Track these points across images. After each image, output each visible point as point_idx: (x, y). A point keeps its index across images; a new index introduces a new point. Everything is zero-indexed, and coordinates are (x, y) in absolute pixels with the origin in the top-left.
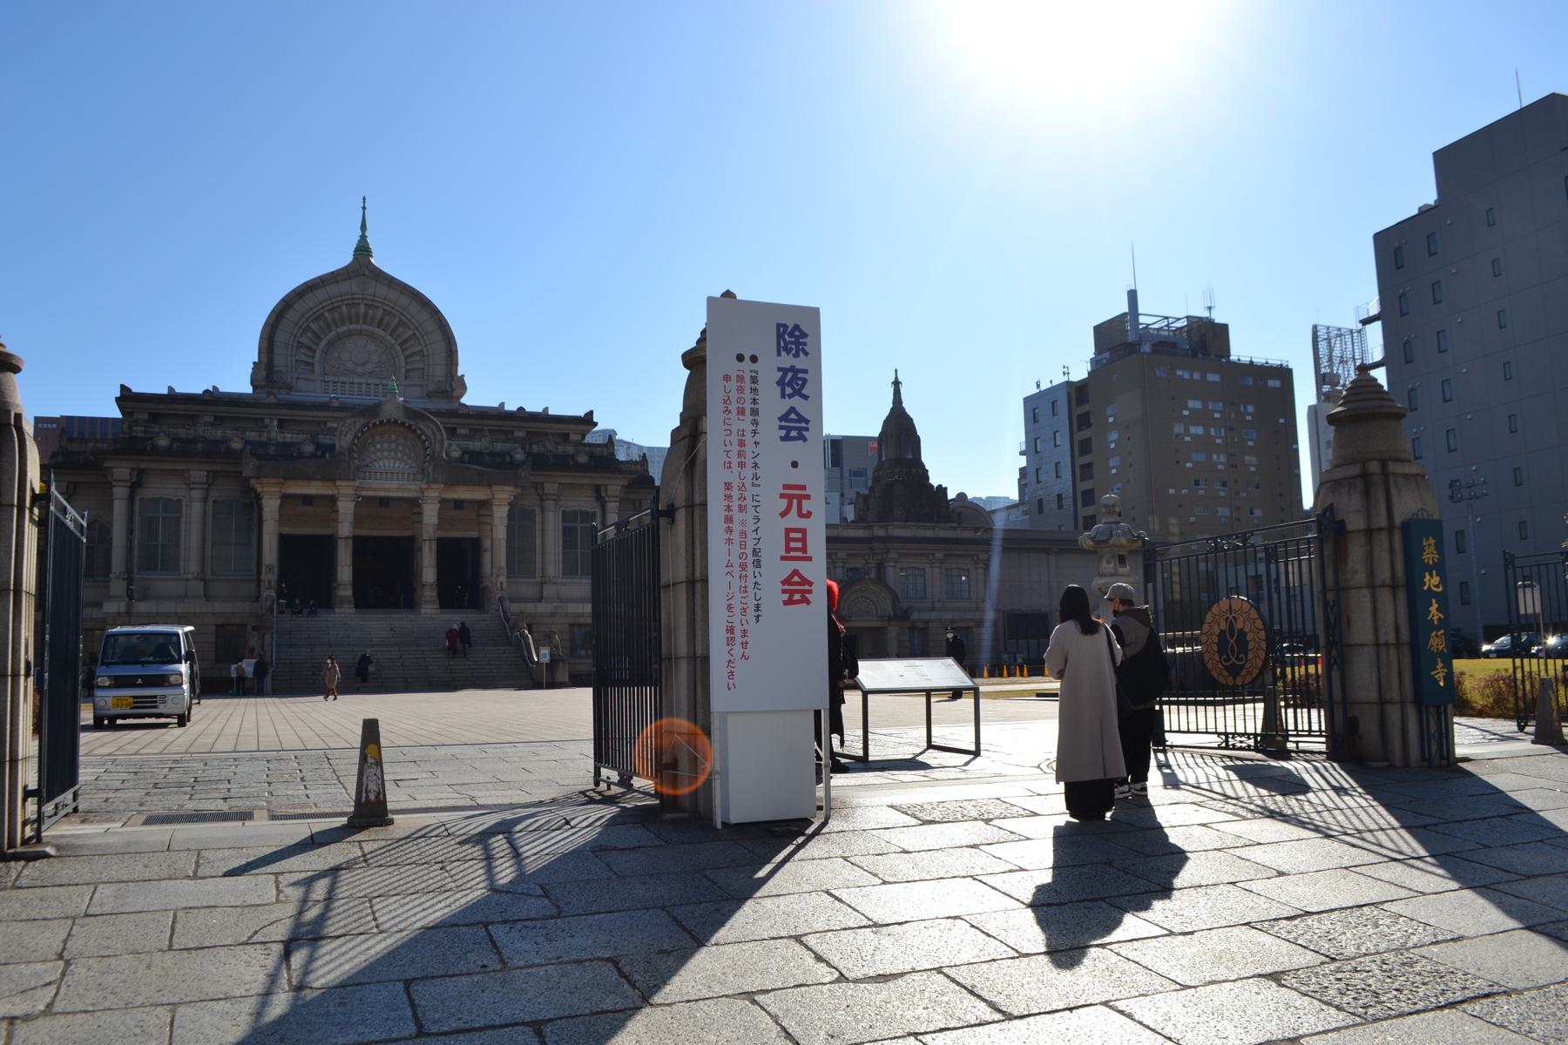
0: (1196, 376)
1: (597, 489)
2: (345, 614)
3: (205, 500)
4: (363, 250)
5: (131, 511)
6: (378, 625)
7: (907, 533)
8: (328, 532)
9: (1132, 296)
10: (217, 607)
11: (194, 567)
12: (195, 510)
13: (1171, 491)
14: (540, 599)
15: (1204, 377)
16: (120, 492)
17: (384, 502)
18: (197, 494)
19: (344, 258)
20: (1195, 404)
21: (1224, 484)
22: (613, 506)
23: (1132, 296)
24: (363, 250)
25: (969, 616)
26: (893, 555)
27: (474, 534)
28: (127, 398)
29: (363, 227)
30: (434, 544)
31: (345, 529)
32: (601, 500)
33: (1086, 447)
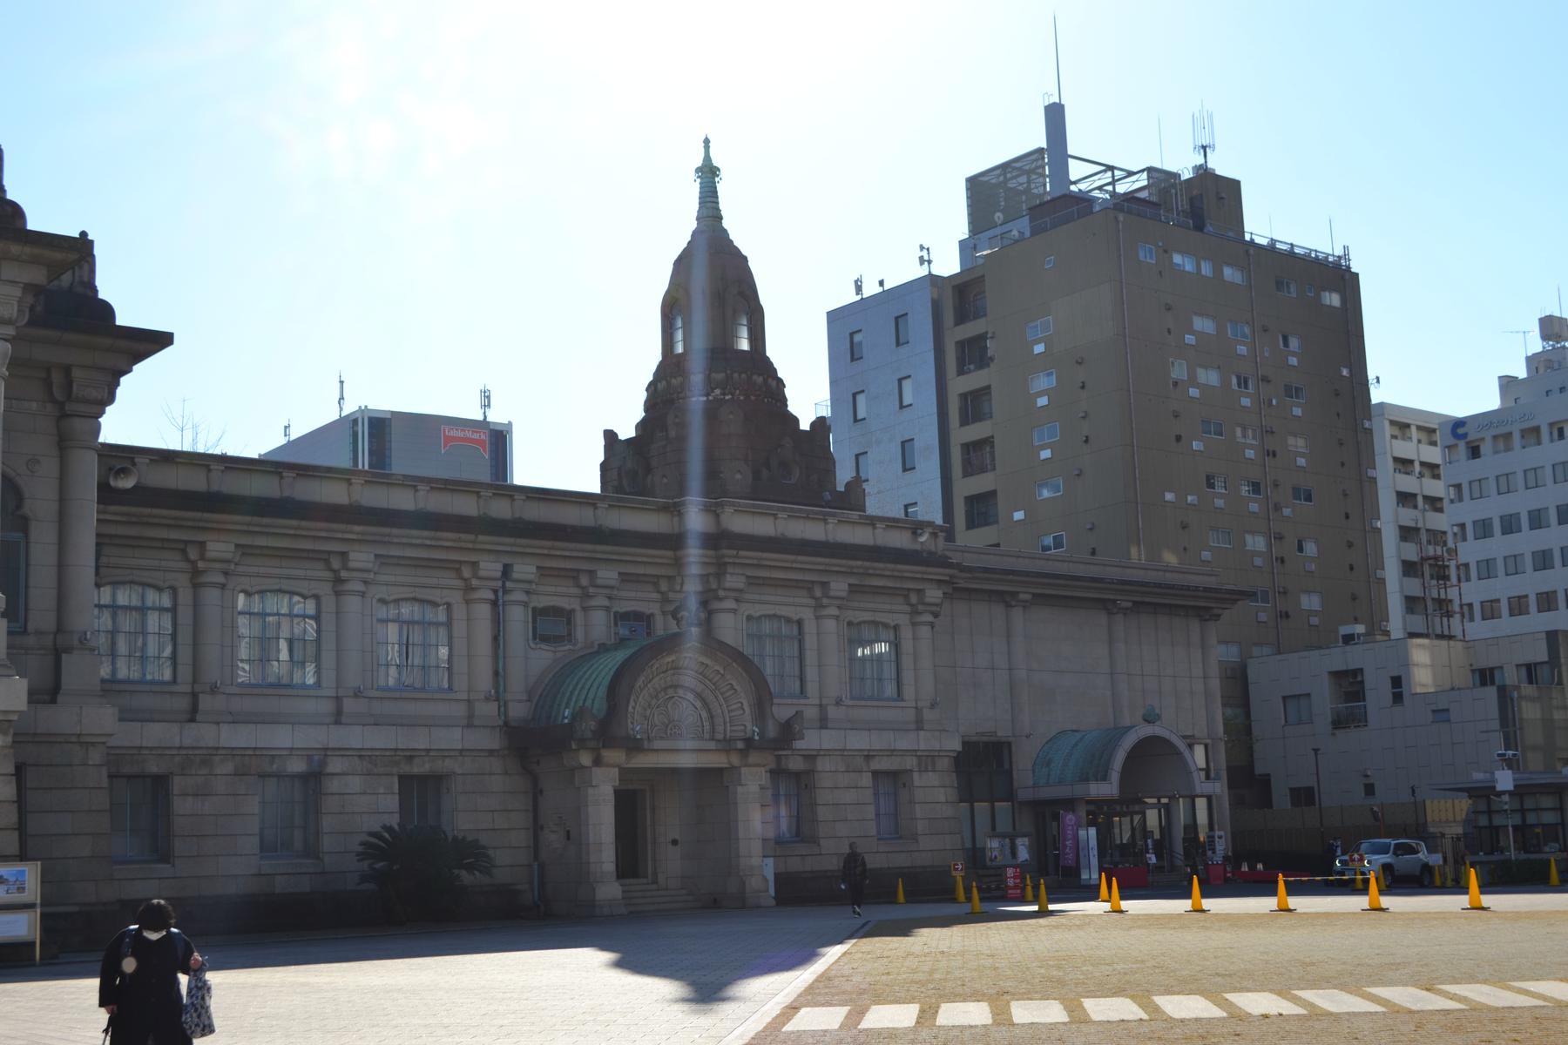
7: (762, 526)
9: (1055, 116)
13: (1169, 496)
15: (1218, 272)
20: (1203, 324)
21: (1256, 487)
23: (1055, 116)
25: (905, 742)
26: (733, 580)
33: (975, 405)
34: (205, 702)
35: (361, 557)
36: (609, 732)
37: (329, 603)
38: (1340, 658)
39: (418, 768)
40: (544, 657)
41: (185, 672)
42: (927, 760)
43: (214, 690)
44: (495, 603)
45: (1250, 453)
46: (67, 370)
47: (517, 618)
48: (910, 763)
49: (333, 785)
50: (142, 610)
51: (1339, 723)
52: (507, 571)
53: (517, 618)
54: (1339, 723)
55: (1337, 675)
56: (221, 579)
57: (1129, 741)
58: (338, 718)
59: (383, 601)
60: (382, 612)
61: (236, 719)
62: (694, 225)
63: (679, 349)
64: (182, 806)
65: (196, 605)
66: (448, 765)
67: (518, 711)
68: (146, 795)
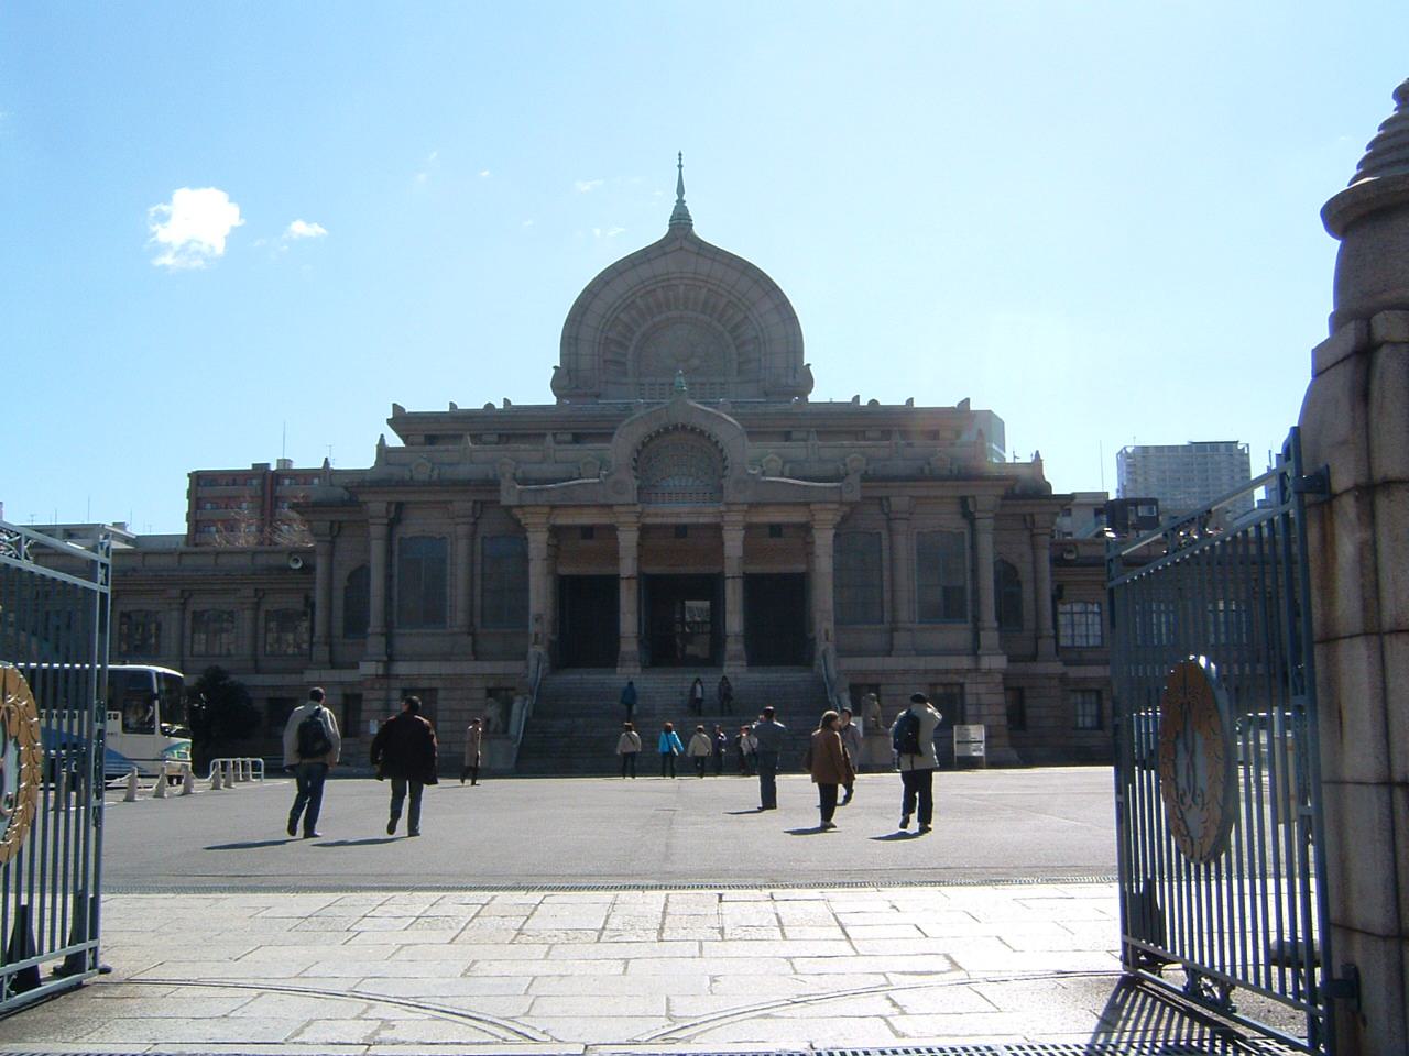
1: (963, 501)
2: (628, 672)
3: (472, 537)
4: (681, 220)
5: (389, 552)
6: (662, 687)
8: (607, 570)
10: (487, 667)
11: (461, 618)
12: (462, 547)
14: (889, 652)
16: (377, 531)
17: (681, 531)
18: (462, 530)
19: (656, 229)
22: (985, 524)
24: (681, 220)
27: (801, 568)
28: (401, 420)
29: (681, 190)
30: (739, 584)
31: (627, 567)
32: (969, 516)
46: (1032, 515)
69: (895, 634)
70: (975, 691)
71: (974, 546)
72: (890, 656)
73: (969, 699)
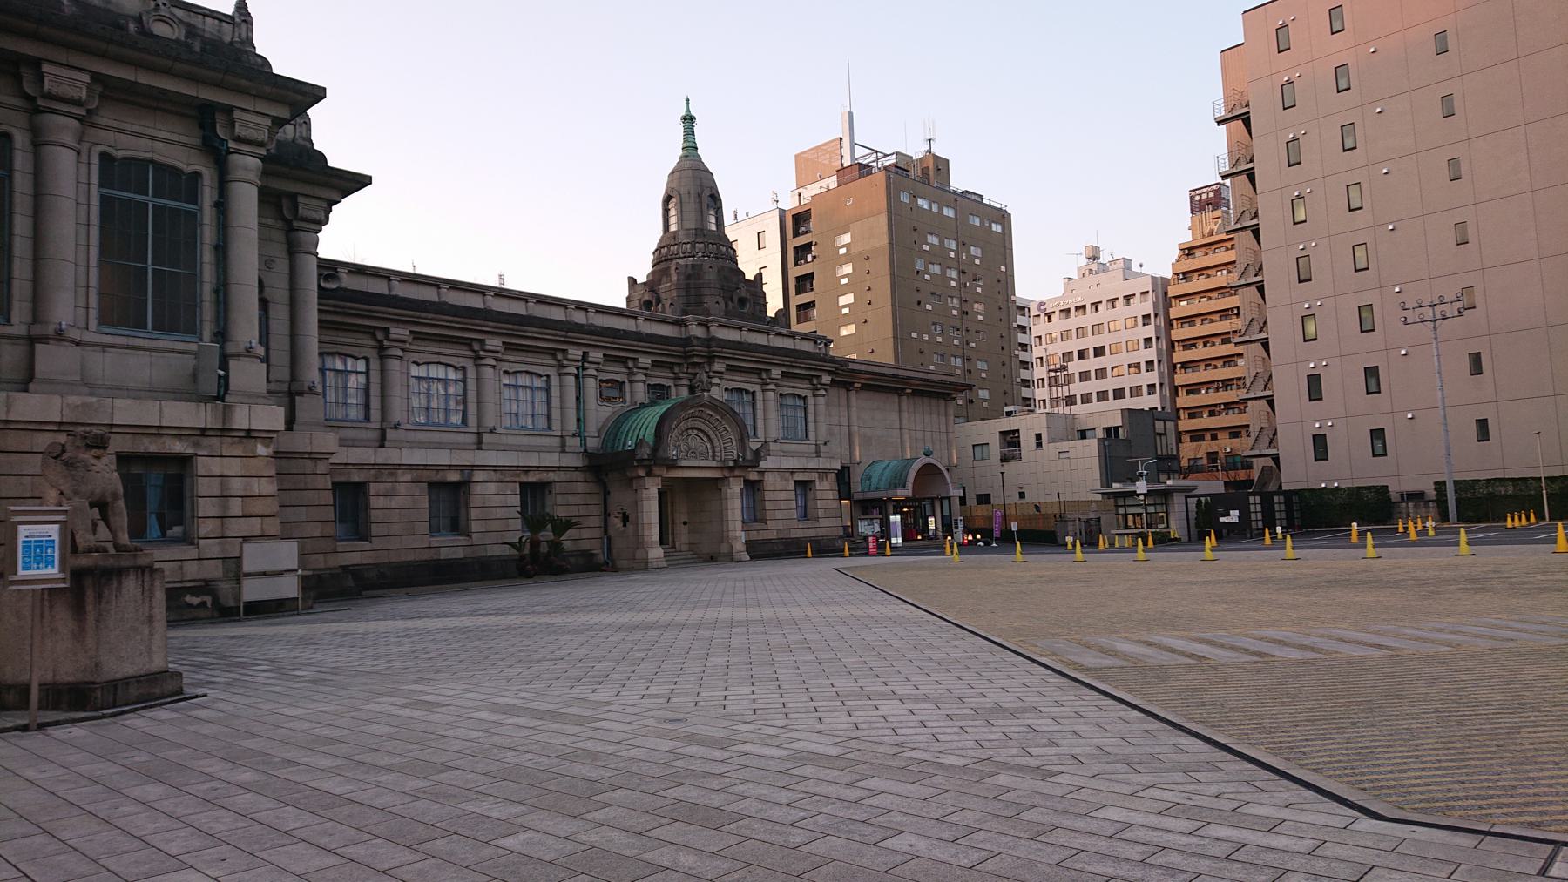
0: (935, 208)
7: (733, 336)
13: (914, 335)
15: (941, 210)
20: (934, 240)
22: (247, 165)
32: (219, 157)
33: (805, 282)
34: (390, 434)
35: (494, 343)
36: (656, 459)
37: (471, 373)
38: (1005, 424)
39: (533, 477)
40: (606, 411)
41: (375, 414)
42: (824, 473)
43: (396, 427)
44: (577, 376)
45: (955, 312)
46: (293, 197)
47: (591, 385)
48: (814, 476)
49: (477, 489)
50: (345, 373)
51: (1005, 459)
52: (585, 354)
53: (591, 385)
54: (1005, 459)
55: (1003, 433)
56: (400, 353)
57: (916, 466)
58: (479, 445)
59: (506, 372)
60: (506, 381)
61: (414, 446)
62: (680, 153)
63: (673, 228)
64: (376, 503)
65: (383, 371)
66: (552, 476)
67: (592, 443)
68: (351, 498)
69: (39, 347)
70: (216, 471)
71: (222, 206)
72: (26, 391)
73: (204, 487)
